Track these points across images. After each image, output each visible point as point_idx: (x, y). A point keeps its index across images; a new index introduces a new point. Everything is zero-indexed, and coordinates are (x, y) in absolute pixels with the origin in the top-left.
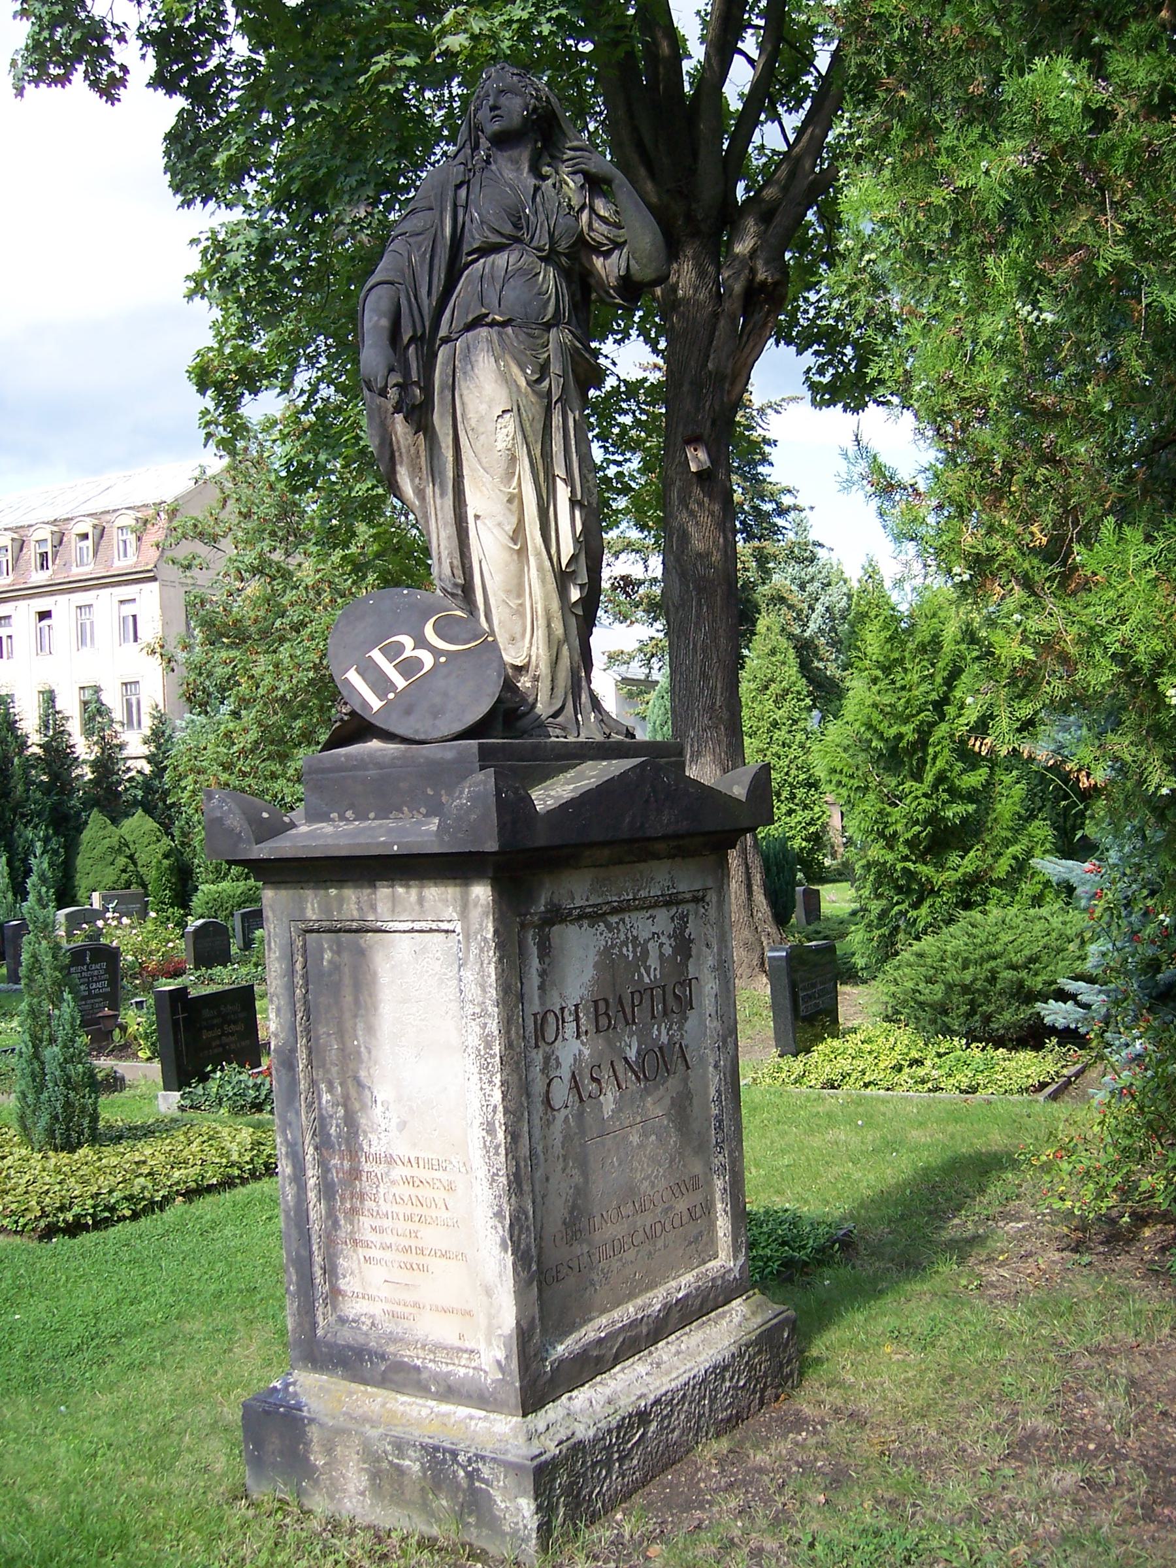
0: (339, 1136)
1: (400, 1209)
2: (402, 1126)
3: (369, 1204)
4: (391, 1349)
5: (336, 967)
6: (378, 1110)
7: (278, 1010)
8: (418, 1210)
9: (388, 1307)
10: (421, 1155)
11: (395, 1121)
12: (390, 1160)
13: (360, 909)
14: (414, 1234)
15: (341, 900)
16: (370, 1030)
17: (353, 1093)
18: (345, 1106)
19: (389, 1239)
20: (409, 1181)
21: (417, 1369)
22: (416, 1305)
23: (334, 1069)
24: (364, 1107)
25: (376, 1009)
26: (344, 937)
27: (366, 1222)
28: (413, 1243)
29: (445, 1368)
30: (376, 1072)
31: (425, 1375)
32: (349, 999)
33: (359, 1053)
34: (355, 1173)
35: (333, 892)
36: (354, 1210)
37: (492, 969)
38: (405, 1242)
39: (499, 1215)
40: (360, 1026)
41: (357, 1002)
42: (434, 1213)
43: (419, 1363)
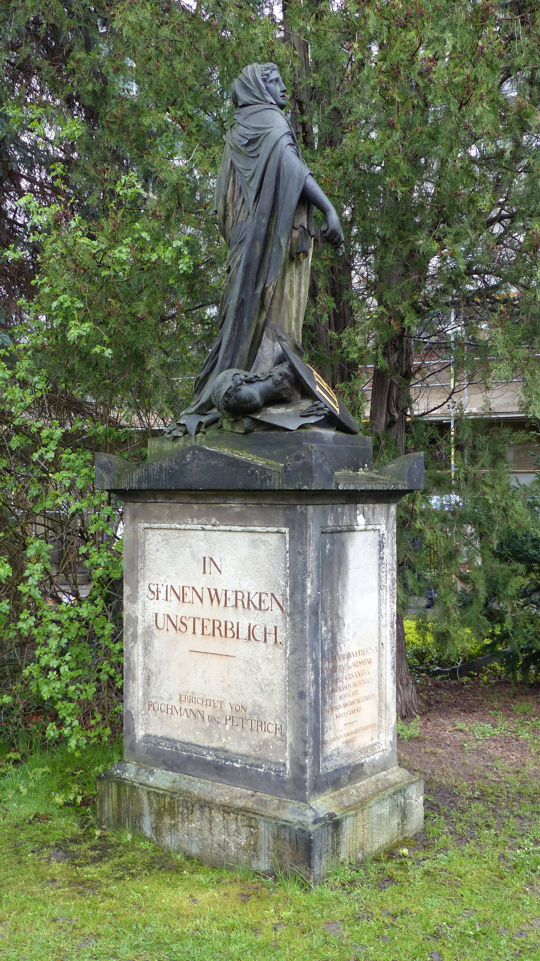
0: (328, 650)
1: (351, 682)
2: (355, 634)
3: (340, 684)
4: (351, 761)
5: (331, 552)
6: (346, 628)
7: (312, 581)
8: (358, 679)
9: (343, 740)
10: (362, 648)
11: (352, 633)
12: (349, 656)
13: (350, 519)
14: (356, 693)
15: (343, 514)
16: (344, 586)
17: (335, 623)
18: (332, 631)
19: (347, 700)
20: (355, 665)
21: (362, 765)
22: (357, 731)
23: (328, 611)
24: (340, 630)
25: (347, 573)
26: (336, 536)
27: (338, 694)
28: (356, 697)
29: (372, 757)
30: (346, 609)
31: (365, 766)
32: (336, 570)
33: (339, 599)
34: (334, 669)
35: (340, 510)
36: (333, 691)
37: (395, 547)
38: (352, 699)
39: (393, 667)
40: (340, 584)
41: (339, 572)
42: (363, 678)
43: (362, 761)
